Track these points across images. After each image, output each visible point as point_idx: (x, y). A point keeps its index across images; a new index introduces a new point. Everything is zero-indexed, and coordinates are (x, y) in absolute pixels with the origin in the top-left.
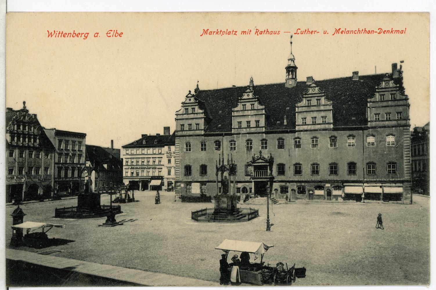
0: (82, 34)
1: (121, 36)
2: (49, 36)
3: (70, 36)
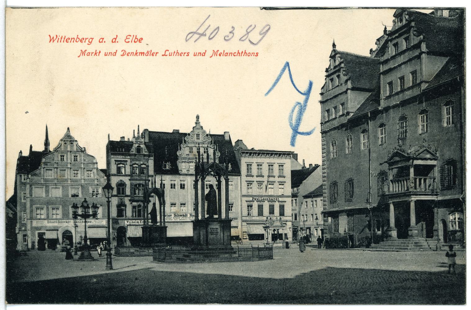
0: (86, 39)
1: (141, 42)
2: (51, 40)
3: (73, 42)
